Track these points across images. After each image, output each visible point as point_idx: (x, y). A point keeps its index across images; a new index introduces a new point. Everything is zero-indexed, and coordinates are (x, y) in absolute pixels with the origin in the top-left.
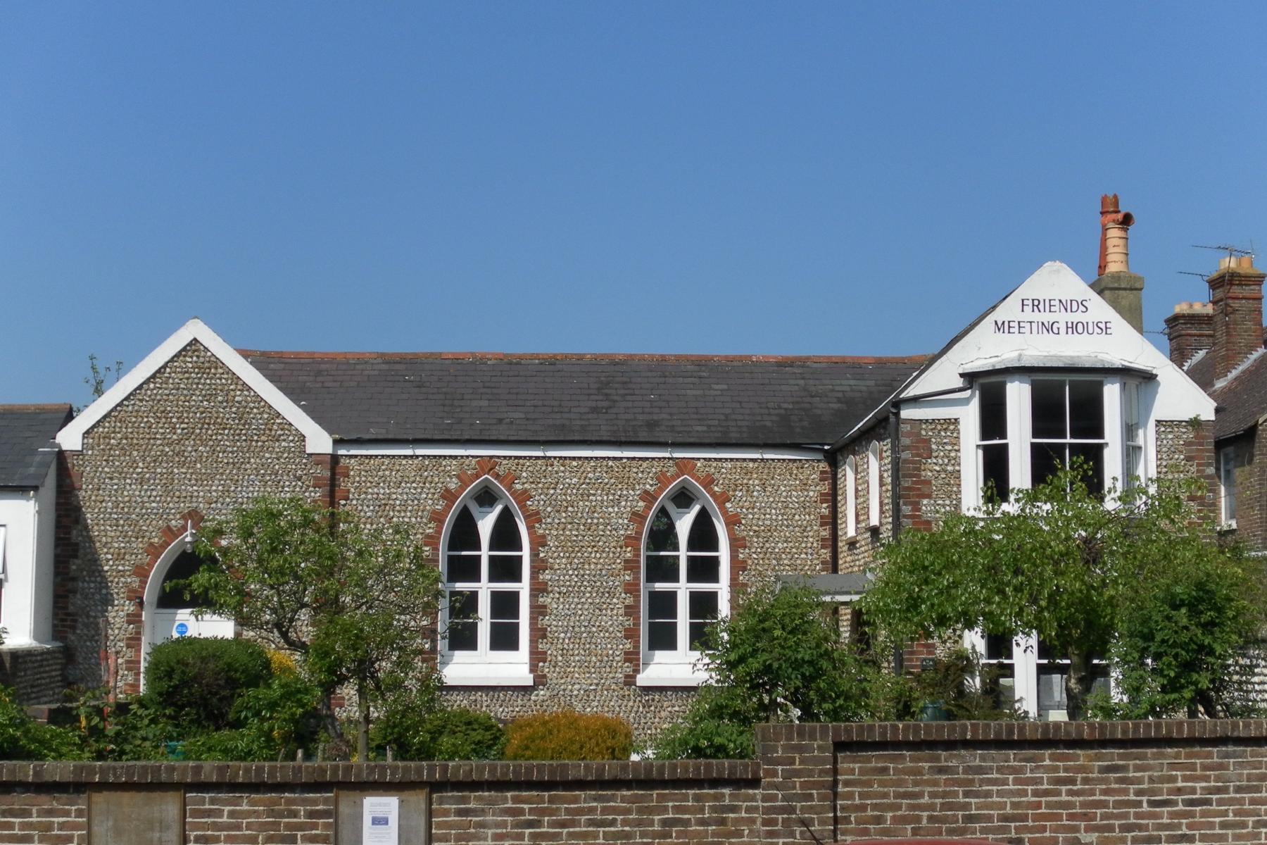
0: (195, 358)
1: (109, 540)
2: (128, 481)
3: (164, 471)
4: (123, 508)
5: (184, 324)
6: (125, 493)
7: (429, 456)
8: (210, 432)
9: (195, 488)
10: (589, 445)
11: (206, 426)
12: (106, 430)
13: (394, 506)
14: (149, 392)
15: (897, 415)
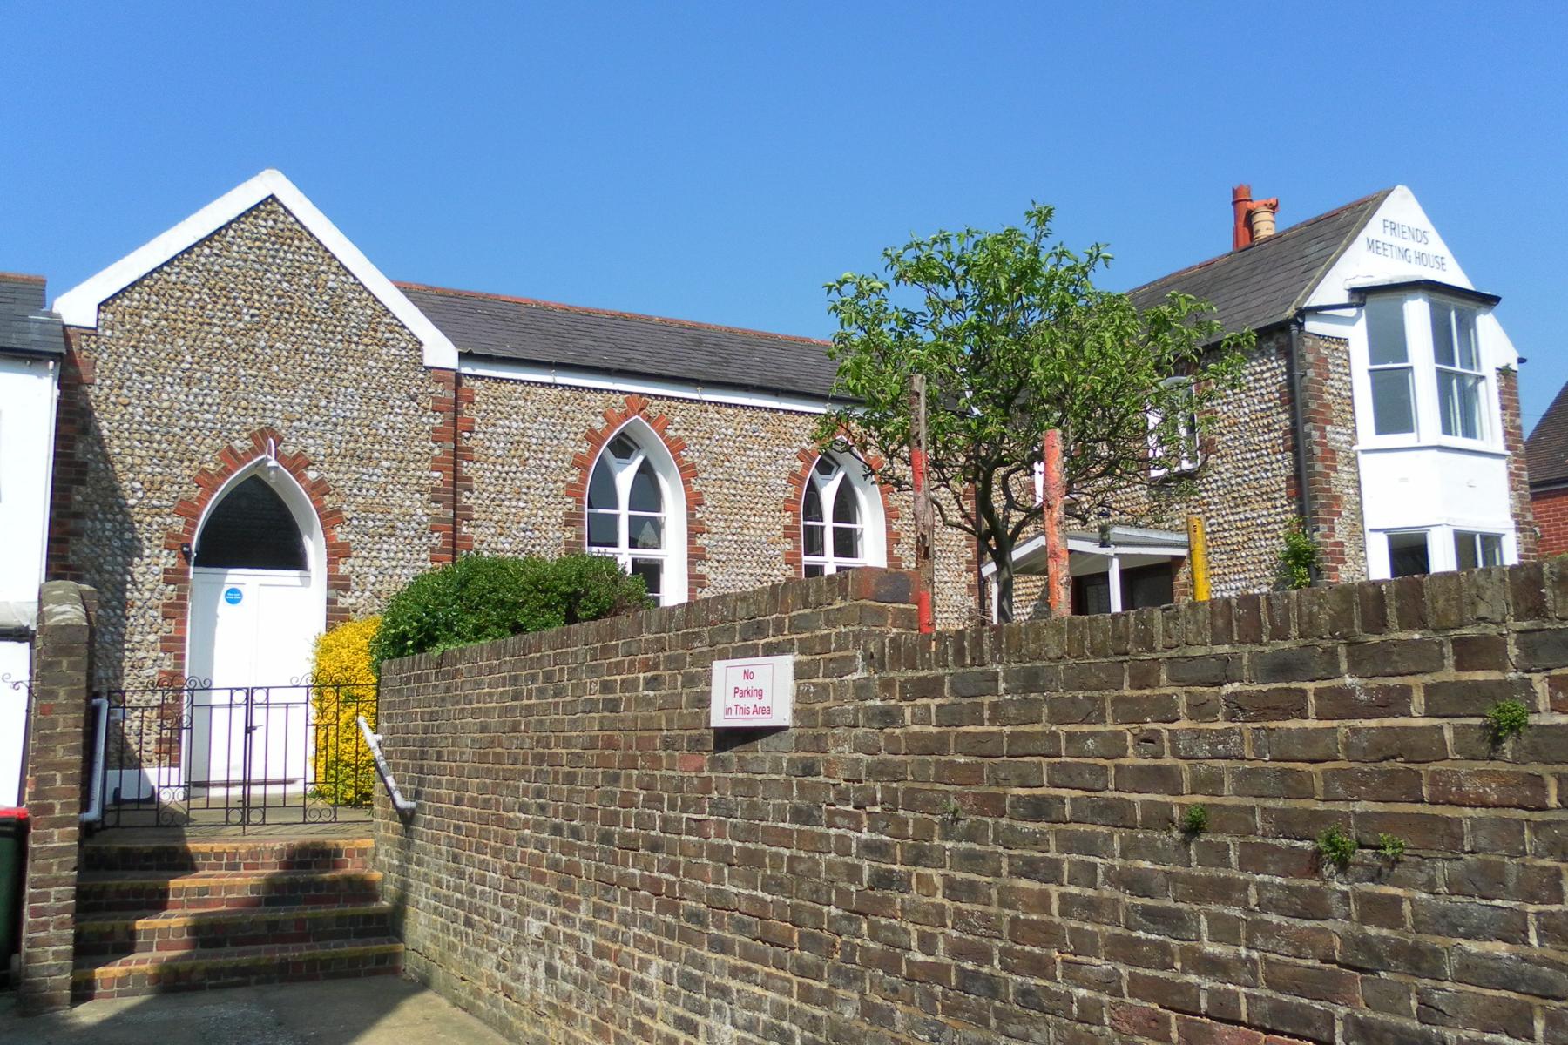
0: (271, 223)
1: (138, 461)
2: (169, 379)
3: (225, 370)
4: (159, 418)
5: (256, 174)
6: (164, 396)
7: (570, 386)
8: (291, 324)
9: (269, 397)
10: (747, 391)
11: (286, 315)
12: (135, 303)
13: (528, 445)
14: (203, 260)
15: (1301, 326)
